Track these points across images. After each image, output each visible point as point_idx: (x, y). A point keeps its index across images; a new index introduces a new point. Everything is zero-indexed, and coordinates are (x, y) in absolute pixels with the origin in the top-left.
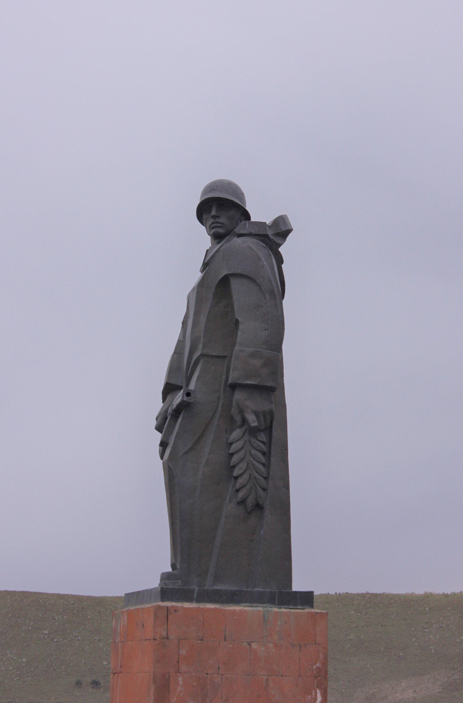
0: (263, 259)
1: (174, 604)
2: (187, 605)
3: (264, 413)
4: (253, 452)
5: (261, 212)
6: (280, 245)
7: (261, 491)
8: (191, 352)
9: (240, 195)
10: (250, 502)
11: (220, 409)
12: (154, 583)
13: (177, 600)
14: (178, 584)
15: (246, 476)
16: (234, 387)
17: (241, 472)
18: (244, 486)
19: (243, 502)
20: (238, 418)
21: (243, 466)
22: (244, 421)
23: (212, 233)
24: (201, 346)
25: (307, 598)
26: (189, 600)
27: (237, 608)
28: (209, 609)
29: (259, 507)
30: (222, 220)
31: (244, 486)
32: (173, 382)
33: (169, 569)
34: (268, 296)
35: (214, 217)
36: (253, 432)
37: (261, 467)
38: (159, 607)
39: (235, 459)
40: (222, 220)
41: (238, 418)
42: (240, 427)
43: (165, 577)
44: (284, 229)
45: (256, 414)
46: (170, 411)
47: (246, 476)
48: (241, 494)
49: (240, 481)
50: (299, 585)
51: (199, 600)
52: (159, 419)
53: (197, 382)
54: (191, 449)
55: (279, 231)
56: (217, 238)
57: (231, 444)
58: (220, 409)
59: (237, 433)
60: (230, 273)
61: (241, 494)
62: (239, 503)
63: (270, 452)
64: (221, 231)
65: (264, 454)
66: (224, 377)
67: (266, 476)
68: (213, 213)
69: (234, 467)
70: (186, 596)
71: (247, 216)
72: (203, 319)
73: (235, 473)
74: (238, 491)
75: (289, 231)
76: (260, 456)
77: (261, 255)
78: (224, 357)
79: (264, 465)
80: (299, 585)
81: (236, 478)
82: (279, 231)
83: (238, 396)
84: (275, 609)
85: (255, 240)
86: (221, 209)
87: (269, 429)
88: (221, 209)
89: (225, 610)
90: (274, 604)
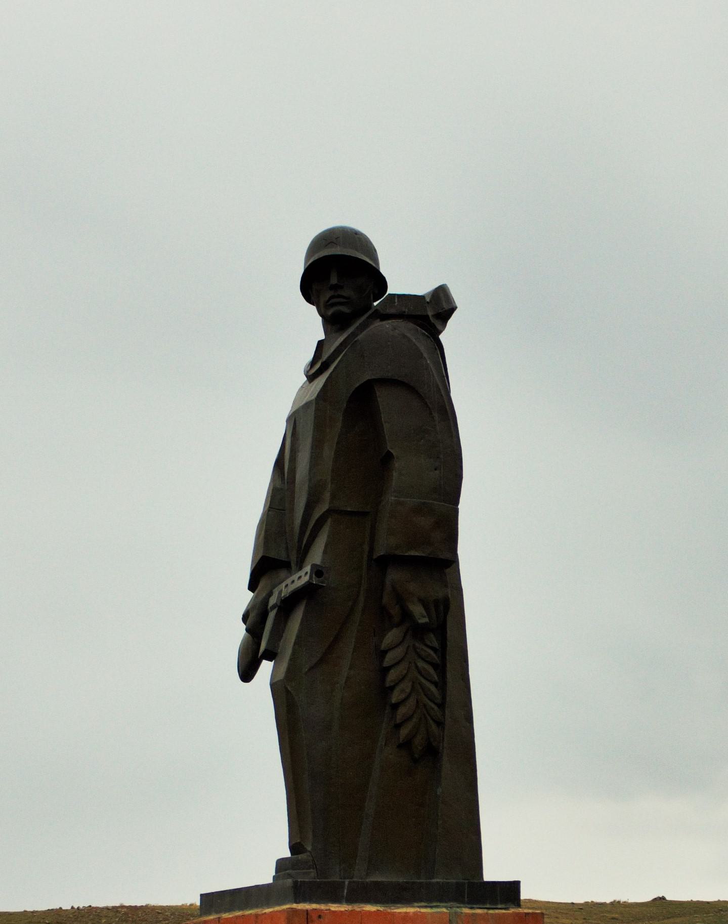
0: (425, 355)
1: (314, 906)
2: (334, 907)
3: (436, 602)
4: (421, 664)
5: (404, 277)
6: (440, 332)
7: (434, 727)
8: (310, 507)
9: (370, 250)
10: (419, 742)
11: (362, 598)
12: (263, 874)
13: (311, 901)
14: (310, 876)
15: (412, 702)
16: (385, 562)
17: (403, 696)
18: (408, 719)
19: (406, 745)
20: (395, 611)
21: (406, 686)
22: (406, 615)
23: (330, 312)
24: (327, 496)
25: (509, 891)
26: (337, 900)
27: (411, 910)
28: (370, 912)
29: (432, 752)
30: (347, 292)
31: (408, 719)
32: (272, 554)
33: (287, 854)
34: (436, 415)
35: (334, 288)
36: (418, 631)
37: (433, 688)
38: (295, 911)
39: (392, 676)
40: (347, 292)
41: (395, 611)
42: (398, 625)
43: (281, 865)
44: (446, 307)
45: (424, 603)
46: (273, 601)
47: (412, 702)
48: (404, 732)
49: (402, 711)
50: (493, 872)
51: (350, 900)
52: (252, 616)
53: (325, 552)
54: (321, 661)
55: (435, 310)
56: (331, 322)
57: (385, 652)
58: (362, 598)
59: (392, 636)
60: (373, 377)
61: (404, 732)
62: (400, 746)
63: (444, 665)
64: (345, 309)
65: (435, 666)
66: (366, 548)
67: (439, 701)
68: (334, 280)
69: (392, 688)
70: (332, 894)
71: (381, 283)
72: (328, 453)
73: (395, 698)
74: (398, 727)
75: (453, 309)
76: (431, 670)
77: (422, 349)
78: (364, 514)
79: (435, 684)
80: (493, 872)
81: (395, 707)
82: (435, 310)
83: (394, 576)
84: (466, 911)
85: (411, 325)
86: (340, 274)
87: (441, 629)
88: (340, 274)
89: (393, 914)
90: (463, 902)
